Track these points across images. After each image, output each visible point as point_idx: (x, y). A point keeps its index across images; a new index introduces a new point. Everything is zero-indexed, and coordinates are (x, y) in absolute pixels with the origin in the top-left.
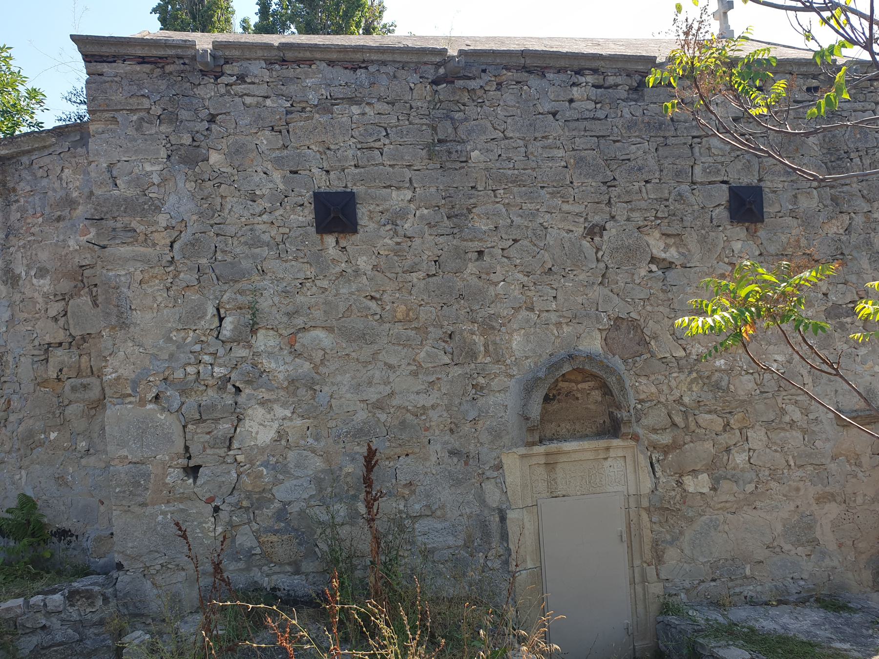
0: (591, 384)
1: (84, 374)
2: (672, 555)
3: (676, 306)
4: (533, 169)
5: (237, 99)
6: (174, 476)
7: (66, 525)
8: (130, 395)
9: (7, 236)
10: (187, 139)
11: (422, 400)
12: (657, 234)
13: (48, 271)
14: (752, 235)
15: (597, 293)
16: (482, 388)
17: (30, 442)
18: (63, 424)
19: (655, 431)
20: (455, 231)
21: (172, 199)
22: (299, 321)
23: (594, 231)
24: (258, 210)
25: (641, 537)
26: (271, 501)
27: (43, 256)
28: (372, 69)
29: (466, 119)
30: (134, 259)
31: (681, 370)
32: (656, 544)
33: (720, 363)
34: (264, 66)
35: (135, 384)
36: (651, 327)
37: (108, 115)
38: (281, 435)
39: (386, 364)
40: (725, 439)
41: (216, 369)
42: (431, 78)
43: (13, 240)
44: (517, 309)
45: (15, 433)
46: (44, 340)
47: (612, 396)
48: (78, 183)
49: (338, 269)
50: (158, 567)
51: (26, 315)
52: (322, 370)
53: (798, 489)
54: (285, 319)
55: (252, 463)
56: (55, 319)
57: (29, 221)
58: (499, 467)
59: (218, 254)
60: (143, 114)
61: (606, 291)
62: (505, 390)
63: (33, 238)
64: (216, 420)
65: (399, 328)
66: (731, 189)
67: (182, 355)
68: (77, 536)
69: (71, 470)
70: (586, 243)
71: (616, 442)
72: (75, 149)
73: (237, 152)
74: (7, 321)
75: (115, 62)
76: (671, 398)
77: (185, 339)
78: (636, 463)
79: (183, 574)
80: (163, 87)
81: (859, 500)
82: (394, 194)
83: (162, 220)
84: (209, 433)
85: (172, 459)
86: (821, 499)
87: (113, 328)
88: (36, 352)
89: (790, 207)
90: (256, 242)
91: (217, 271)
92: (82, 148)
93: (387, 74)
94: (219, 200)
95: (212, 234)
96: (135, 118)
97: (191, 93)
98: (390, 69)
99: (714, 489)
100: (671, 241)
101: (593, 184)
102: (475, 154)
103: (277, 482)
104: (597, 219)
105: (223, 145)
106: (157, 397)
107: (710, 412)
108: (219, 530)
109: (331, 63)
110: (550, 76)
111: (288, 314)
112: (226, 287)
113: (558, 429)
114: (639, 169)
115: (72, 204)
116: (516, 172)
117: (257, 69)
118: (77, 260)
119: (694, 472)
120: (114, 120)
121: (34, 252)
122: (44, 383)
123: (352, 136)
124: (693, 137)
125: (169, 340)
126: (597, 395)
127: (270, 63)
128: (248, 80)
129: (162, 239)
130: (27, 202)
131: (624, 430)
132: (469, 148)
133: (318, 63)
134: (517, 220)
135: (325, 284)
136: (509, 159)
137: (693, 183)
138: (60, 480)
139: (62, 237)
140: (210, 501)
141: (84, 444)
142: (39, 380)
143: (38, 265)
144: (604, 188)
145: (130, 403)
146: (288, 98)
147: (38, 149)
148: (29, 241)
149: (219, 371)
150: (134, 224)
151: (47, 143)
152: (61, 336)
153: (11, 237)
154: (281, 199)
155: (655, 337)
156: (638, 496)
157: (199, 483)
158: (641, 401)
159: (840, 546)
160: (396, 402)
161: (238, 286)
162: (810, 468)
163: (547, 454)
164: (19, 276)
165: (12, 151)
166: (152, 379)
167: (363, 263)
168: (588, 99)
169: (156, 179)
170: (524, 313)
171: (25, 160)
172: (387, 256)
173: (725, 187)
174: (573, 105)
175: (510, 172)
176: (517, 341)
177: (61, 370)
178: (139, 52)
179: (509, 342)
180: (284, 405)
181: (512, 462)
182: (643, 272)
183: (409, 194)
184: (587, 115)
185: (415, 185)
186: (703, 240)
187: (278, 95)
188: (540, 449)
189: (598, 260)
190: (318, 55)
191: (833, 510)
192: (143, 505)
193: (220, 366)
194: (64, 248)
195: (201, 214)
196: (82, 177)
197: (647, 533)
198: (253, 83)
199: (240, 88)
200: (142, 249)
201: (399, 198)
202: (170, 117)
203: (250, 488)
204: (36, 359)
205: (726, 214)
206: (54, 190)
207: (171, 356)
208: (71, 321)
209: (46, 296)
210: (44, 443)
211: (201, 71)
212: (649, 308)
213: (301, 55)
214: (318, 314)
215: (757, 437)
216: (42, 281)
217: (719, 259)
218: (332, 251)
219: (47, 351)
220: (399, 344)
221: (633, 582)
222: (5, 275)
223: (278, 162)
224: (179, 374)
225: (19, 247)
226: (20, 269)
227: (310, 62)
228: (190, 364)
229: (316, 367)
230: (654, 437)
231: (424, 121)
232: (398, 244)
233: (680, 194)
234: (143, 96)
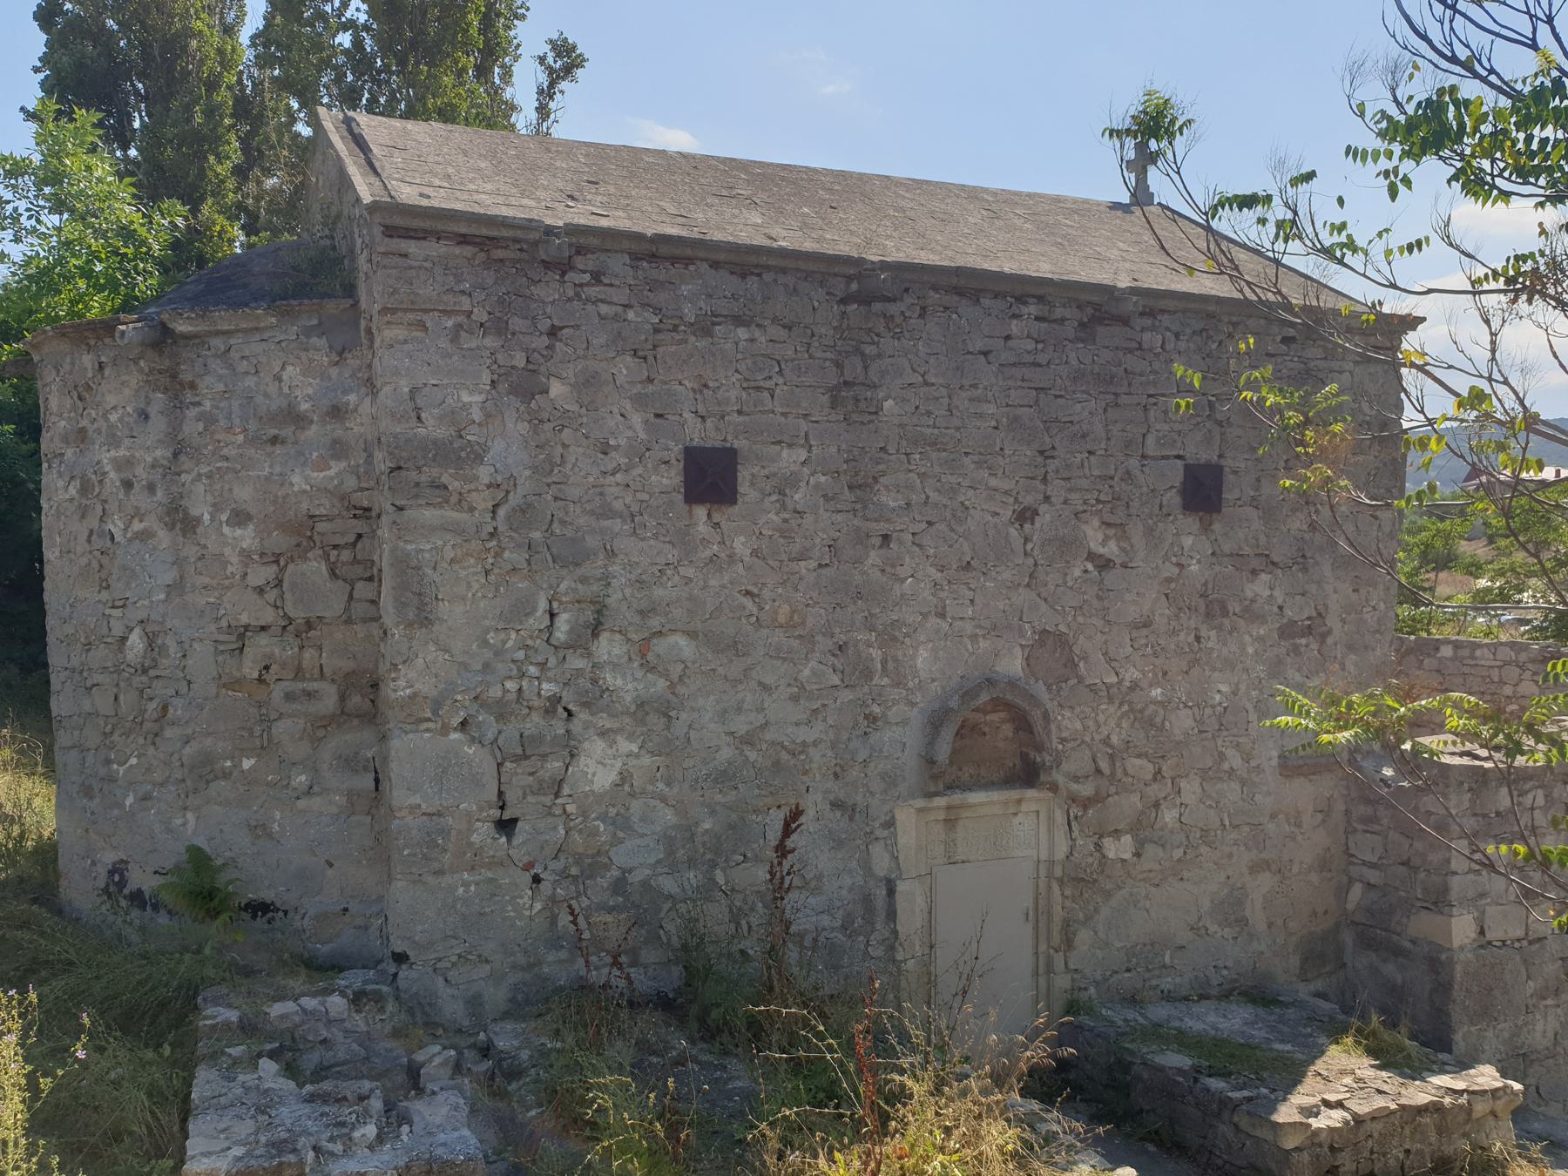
0: (1002, 715)
1: (308, 676)
2: (1083, 937)
3: (1111, 617)
4: (958, 429)
5: (590, 307)
6: (483, 832)
7: (267, 895)
8: (428, 720)
9: (176, 455)
10: (519, 360)
11: (805, 734)
12: (1096, 523)
13: (249, 517)
14: (1206, 528)
15: (1023, 597)
16: (875, 719)
17: (205, 771)
18: (265, 749)
19: (1076, 779)
20: (858, 506)
21: (497, 446)
22: (655, 622)
23: (1025, 516)
24: (610, 467)
25: (1049, 915)
26: (607, 867)
27: (244, 494)
28: (768, 277)
29: (879, 356)
30: (444, 528)
31: (1111, 700)
32: (1066, 924)
33: (1157, 692)
34: (628, 262)
35: (437, 705)
36: (1082, 644)
37: (411, 316)
38: (624, 777)
39: (760, 683)
40: (1155, 791)
41: (545, 686)
42: (840, 294)
43: (185, 462)
44: (925, 616)
45: (176, 756)
46: (238, 620)
47: (1031, 732)
48: (310, 391)
49: (708, 553)
50: (454, 959)
51: (207, 580)
52: (681, 690)
53: (1230, 856)
54: (637, 619)
55: (584, 814)
56: (260, 590)
57: (217, 437)
58: (890, 824)
59: (555, 525)
60: (461, 319)
61: (1033, 595)
62: (904, 723)
63: (226, 464)
64: (544, 757)
65: (778, 636)
66: (1187, 467)
67: (500, 665)
68: (286, 913)
69: (278, 815)
70: (1013, 532)
71: (1031, 793)
72: (308, 337)
73: (587, 384)
74: (168, 586)
75: (424, 238)
76: (1097, 737)
77: (504, 642)
78: (1051, 820)
79: (488, 967)
80: (490, 281)
81: (1295, 869)
82: (785, 453)
83: (484, 473)
84: (532, 774)
85: (481, 809)
86: (1255, 869)
87: (410, 625)
88: (221, 638)
89: (1252, 493)
90: (606, 513)
91: (554, 550)
92: (319, 337)
93: (786, 286)
94: (559, 449)
95: (549, 497)
96: (450, 323)
97: (528, 292)
98: (790, 280)
99: (1137, 855)
100: (1111, 532)
101: (1028, 453)
102: (888, 404)
103: (616, 842)
104: (1028, 500)
105: (569, 372)
106: (463, 723)
107: (1139, 756)
108: (538, 906)
109: (715, 265)
110: (986, 302)
111: (641, 612)
112: (564, 572)
113: (960, 773)
114: (1084, 436)
115: (300, 420)
116: (936, 431)
117: (618, 265)
118: (304, 506)
119: (1116, 834)
120: (422, 326)
121: (227, 487)
122: (236, 684)
123: (737, 371)
124: (1150, 396)
125: (485, 643)
126: (1007, 730)
127: (635, 257)
128: (606, 281)
129: (482, 501)
130: (217, 408)
131: (1043, 778)
132: (881, 395)
133: (698, 263)
134: (934, 496)
135: (690, 572)
136: (929, 413)
137: (1144, 457)
138: (260, 830)
139: (278, 469)
140: (528, 866)
141: (303, 778)
142: (225, 679)
143: (234, 506)
144: (1040, 459)
145: (427, 730)
146: (657, 310)
147: (245, 331)
148: (219, 468)
149: (548, 688)
150: (445, 479)
151: (262, 325)
152: (269, 616)
153: (182, 458)
154: (639, 452)
155: (1085, 658)
156: (1051, 863)
157: (515, 842)
158: (1063, 740)
159: (1270, 925)
160: (769, 735)
161: (580, 571)
162: (1246, 829)
163: (949, 808)
164: (198, 520)
165: (199, 328)
166: (459, 697)
167: (740, 545)
168: (1028, 337)
169: (477, 415)
170: (933, 621)
171: (218, 343)
172: (771, 537)
173: (1180, 463)
174: (1011, 343)
175: (929, 431)
176: (923, 658)
177: (267, 668)
178: (463, 229)
179: (914, 657)
180: (631, 737)
181: (906, 817)
182: (1077, 573)
183: (803, 455)
184: (1029, 358)
185: (812, 443)
186: (1150, 531)
187: (643, 305)
188: (940, 802)
189: (1026, 554)
190: (701, 254)
191: (1266, 881)
192: (439, 873)
193: (549, 681)
194: (282, 485)
195: (535, 469)
196: (318, 381)
197: (1057, 909)
198: (611, 285)
199: (593, 291)
200: (455, 515)
201: (790, 458)
202: (498, 326)
203: (581, 850)
204: (221, 648)
205: (1178, 500)
206: (266, 395)
207: (486, 666)
208: (288, 596)
209: (246, 555)
210: (231, 773)
211: (543, 261)
212: (1080, 619)
213: (678, 252)
214: (677, 612)
215: (1190, 789)
216: (239, 532)
217: (1166, 558)
218: (703, 528)
219: (241, 636)
220: (778, 658)
221: (1036, 973)
222: (168, 514)
223: (640, 401)
224: (495, 692)
225: (199, 475)
226: (201, 510)
227: (689, 261)
228: (510, 678)
229: (672, 685)
230: (1074, 787)
231: (829, 355)
232: (785, 521)
233: (1128, 472)
234: (463, 292)
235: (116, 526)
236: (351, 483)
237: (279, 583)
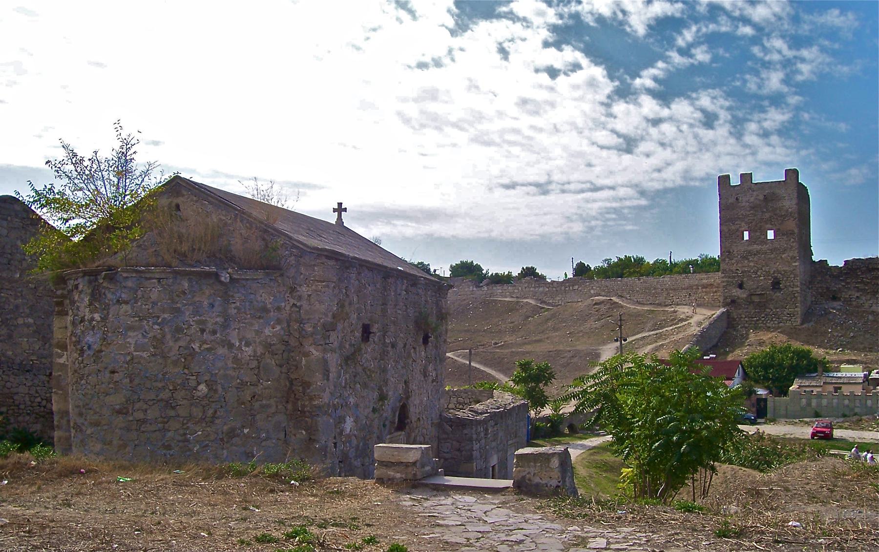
23: (405, 346)
27: (250, 335)
45: (220, 430)
109: (367, 267)
177: (254, 397)
204: (239, 390)
216: (247, 349)
235: (196, 346)
236: (282, 333)
237: (259, 368)
